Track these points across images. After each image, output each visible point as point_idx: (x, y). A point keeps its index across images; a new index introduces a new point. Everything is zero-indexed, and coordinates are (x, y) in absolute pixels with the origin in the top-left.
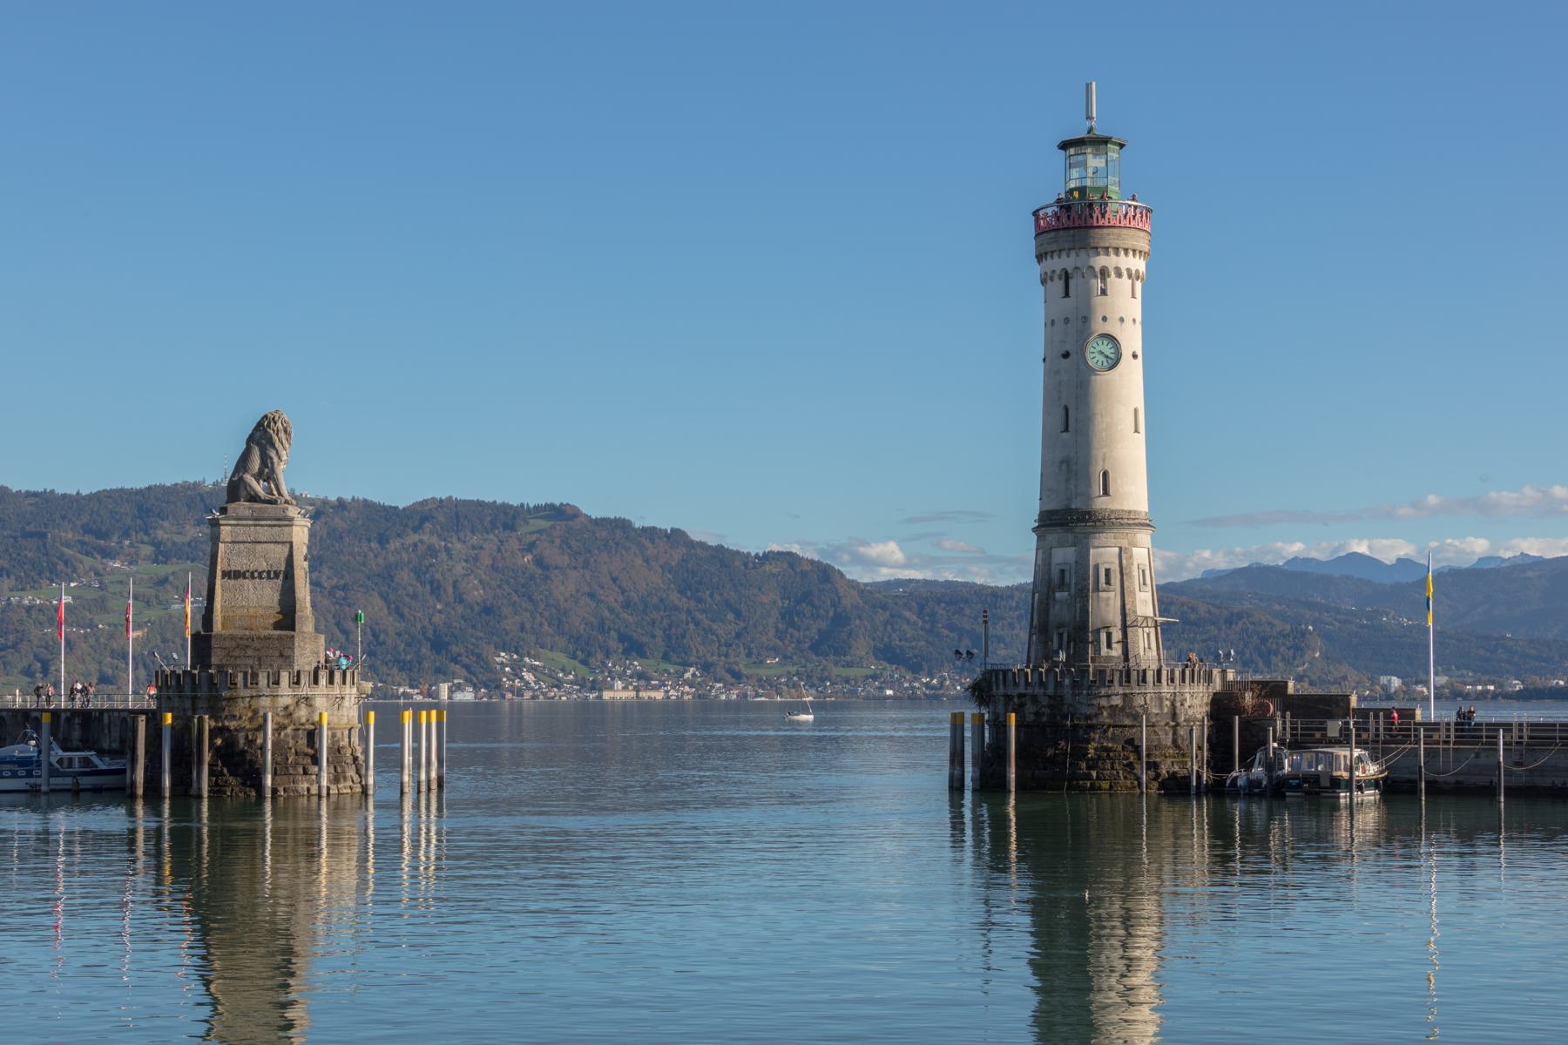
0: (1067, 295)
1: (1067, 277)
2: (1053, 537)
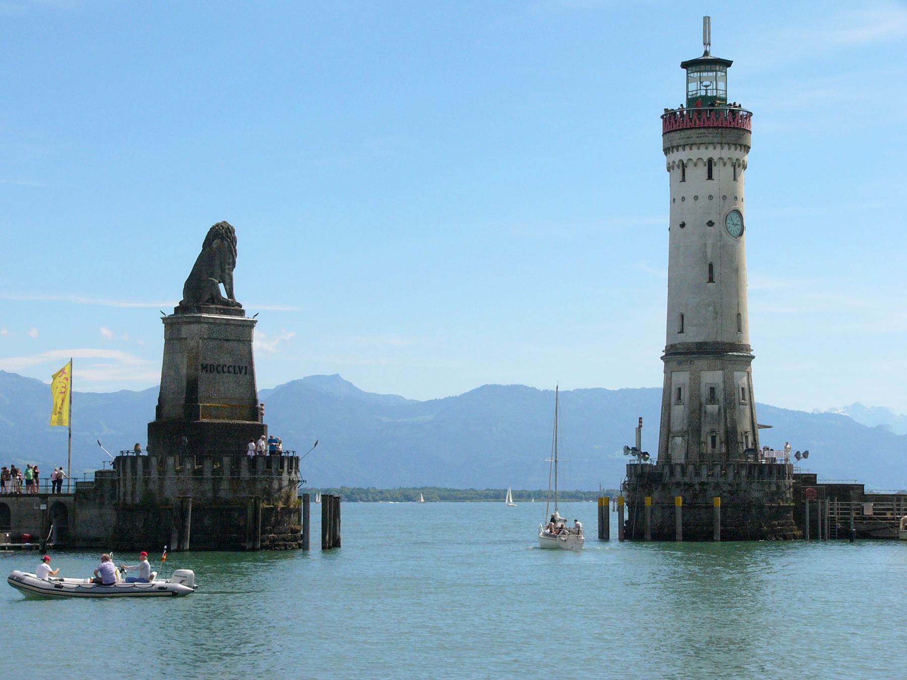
0: (710, 177)
1: (710, 163)
2: (701, 363)
